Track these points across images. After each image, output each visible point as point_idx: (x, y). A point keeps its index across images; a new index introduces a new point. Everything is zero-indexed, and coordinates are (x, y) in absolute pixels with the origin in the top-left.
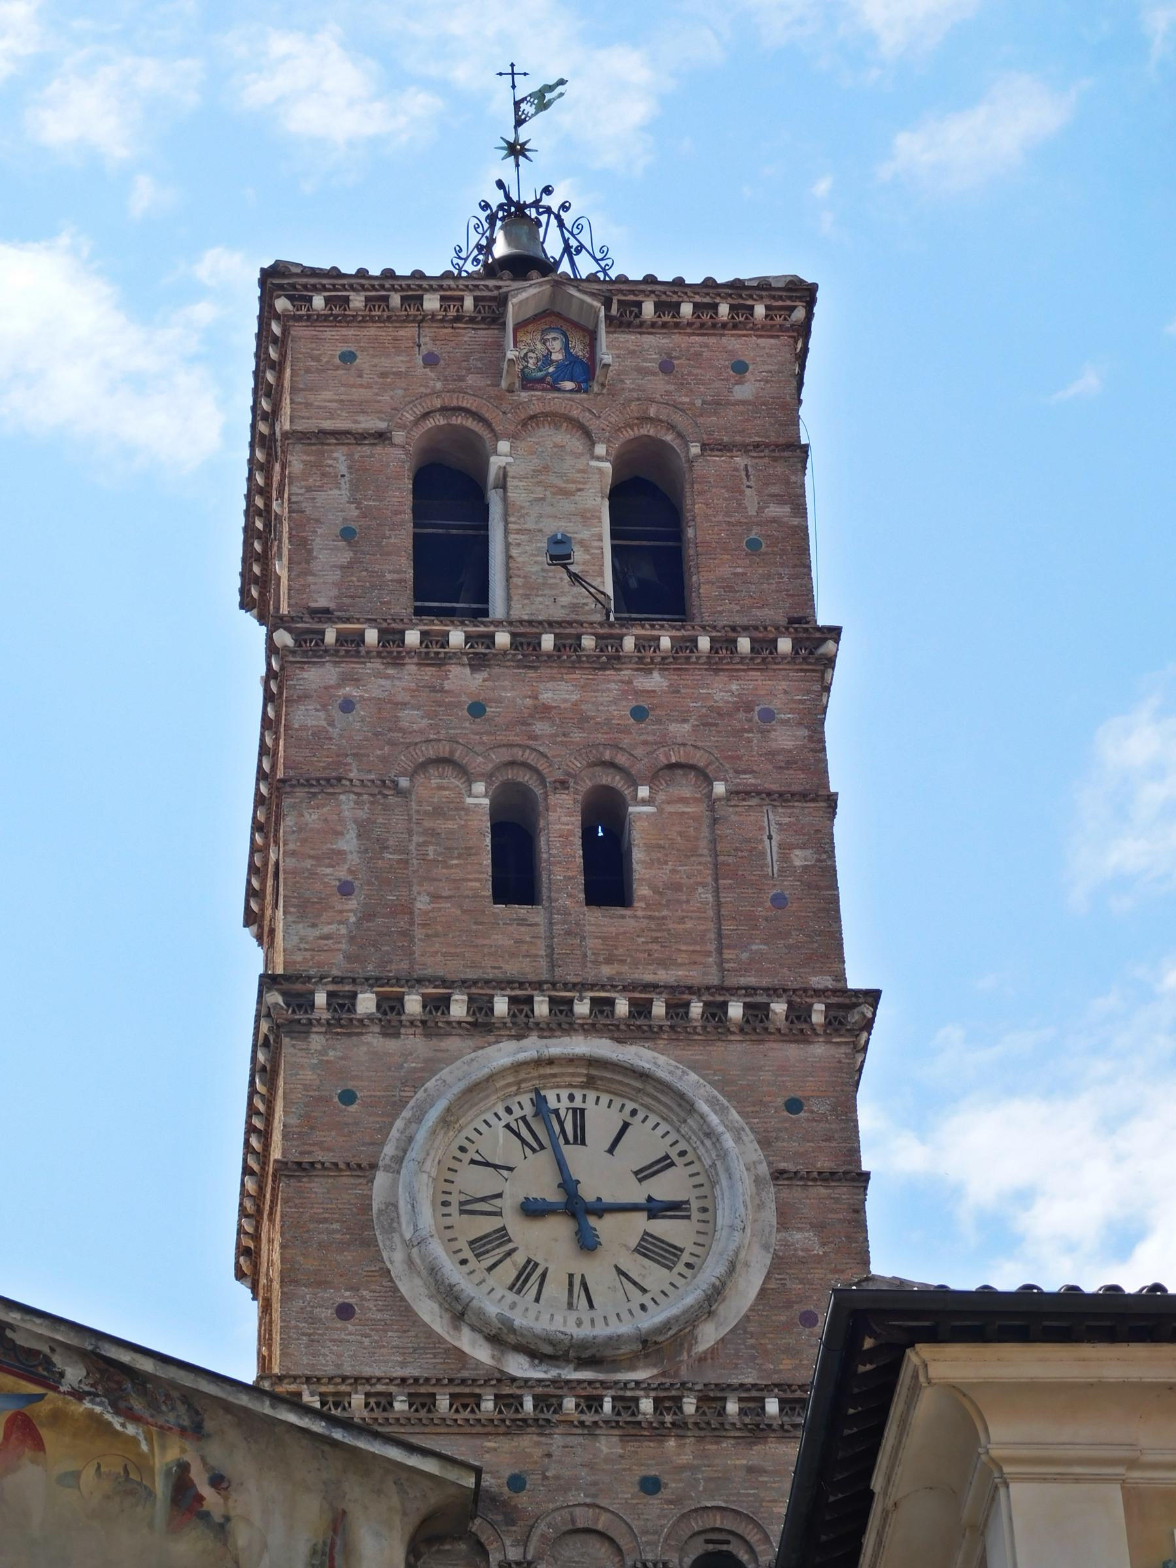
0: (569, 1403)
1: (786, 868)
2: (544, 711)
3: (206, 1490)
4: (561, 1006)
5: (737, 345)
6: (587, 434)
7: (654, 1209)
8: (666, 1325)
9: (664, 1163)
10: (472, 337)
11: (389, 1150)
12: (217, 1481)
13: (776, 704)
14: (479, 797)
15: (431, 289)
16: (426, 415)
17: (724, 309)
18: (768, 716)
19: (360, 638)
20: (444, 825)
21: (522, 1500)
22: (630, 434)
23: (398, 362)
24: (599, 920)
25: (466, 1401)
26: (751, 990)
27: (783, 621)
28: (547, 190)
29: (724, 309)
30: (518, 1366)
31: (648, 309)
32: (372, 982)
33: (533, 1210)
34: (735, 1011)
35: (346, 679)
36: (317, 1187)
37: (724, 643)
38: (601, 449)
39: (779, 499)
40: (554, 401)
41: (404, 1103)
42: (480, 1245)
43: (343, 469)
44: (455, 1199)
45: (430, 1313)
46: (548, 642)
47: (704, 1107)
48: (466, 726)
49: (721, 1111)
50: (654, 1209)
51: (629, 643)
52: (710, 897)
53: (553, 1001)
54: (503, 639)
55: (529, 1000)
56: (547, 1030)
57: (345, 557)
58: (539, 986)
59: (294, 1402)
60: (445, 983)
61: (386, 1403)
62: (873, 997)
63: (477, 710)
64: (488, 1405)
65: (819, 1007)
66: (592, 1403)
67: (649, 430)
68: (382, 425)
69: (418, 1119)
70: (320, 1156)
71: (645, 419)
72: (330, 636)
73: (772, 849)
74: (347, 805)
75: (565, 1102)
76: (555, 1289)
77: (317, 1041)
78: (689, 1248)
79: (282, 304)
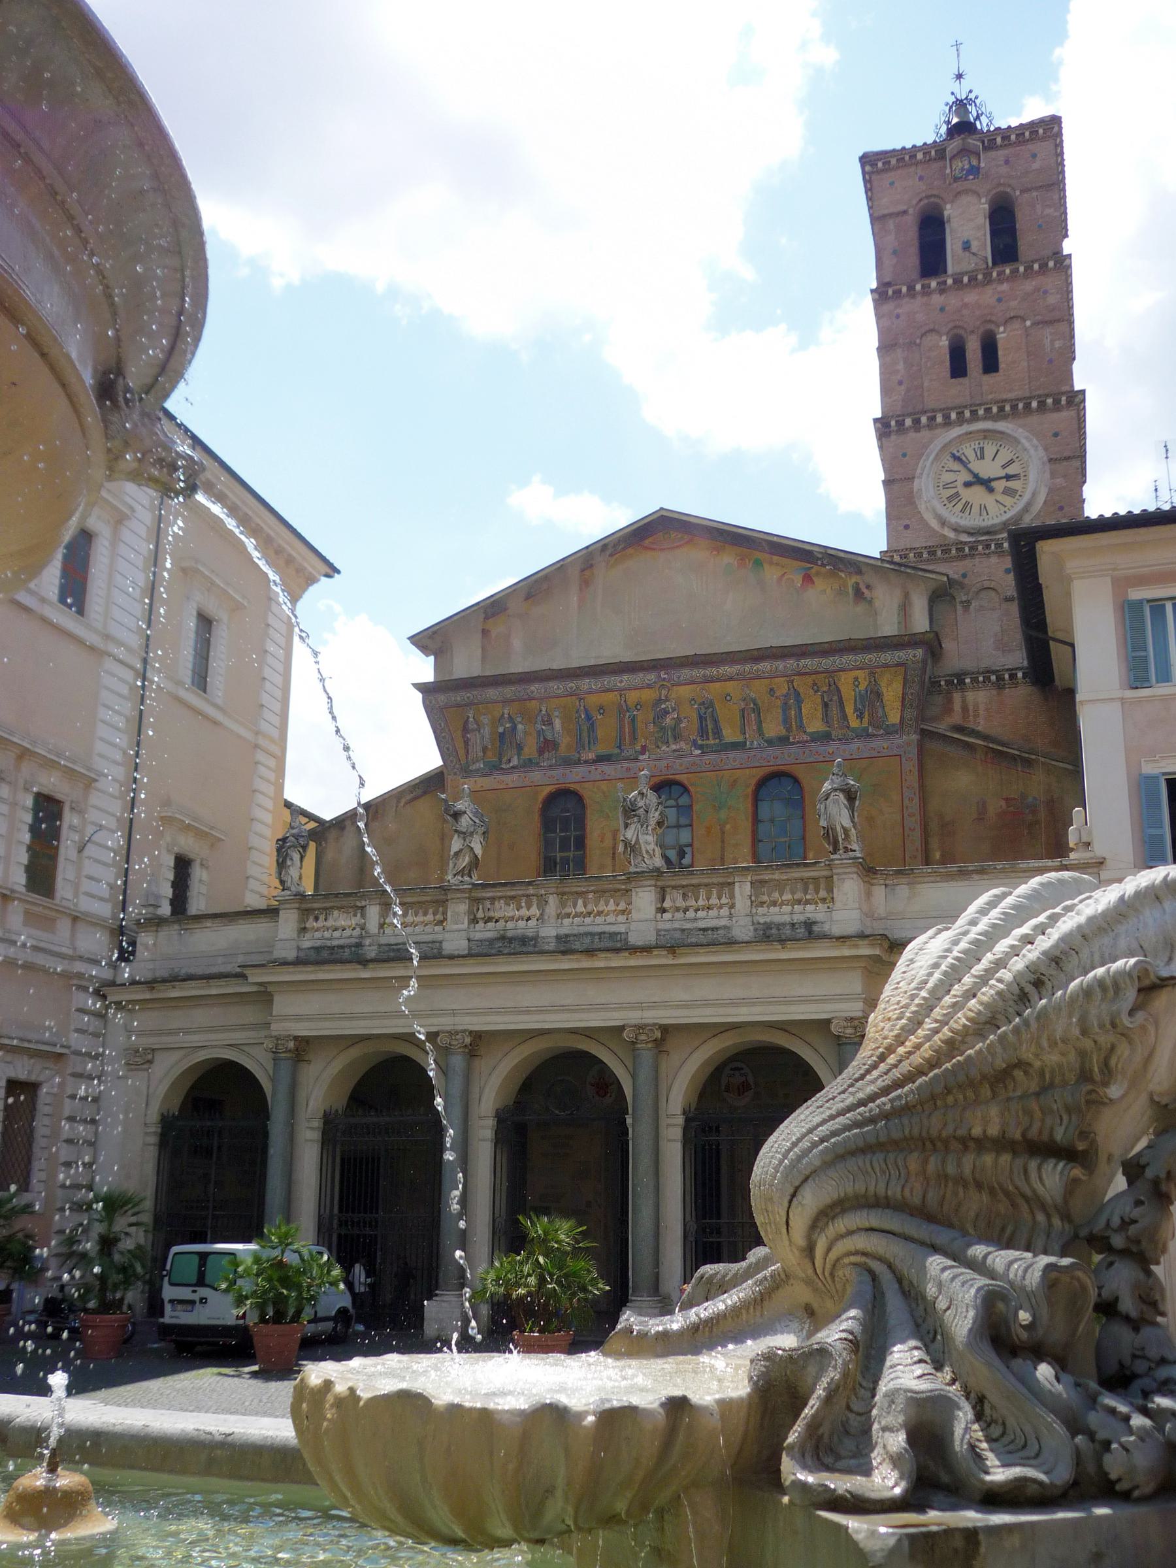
0: (980, 548)
2: (966, 305)
3: (865, 590)
4: (974, 413)
5: (1031, 147)
6: (978, 195)
7: (1008, 477)
8: (1011, 518)
9: (1011, 462)
10: (936, 165)
11: (919, 471)
12: (868, 587)
14: (944, 342)
15: (919, 151)
16: (921, 200)
17: (1027, 134)
18: (1045, 292)
19: (900, 291)
21: (966, 581)
22: (994, 192)
24: (989, 379)
25: (946, 551)
26: (1039, 396)
27: (1051, 254)
28: (971, 91)
29: (1027, 134)
30: (965, 538)
31: (999, 140)
32: (909, 415)
33: (967, 485)
34: (1034, 404)
36: (896, 487)
37: (1029, 268)
38: (983, 200)
39: (1049, 206)
40: (966, 185)
42: (950, 499)
43: (892, 227)
44: (941, 485)
46: (966, 279)
47: (1023, 441)
49: (1030, 440)
50: (1008, 477)
51: (995, 274)
52: (1026, 364)
53: (971, 411)
54: (950, 281)
55: (963, 412)
56: (969, 421)
57: (895, 261)
58: (965, 407)
60: (933, 411)
61: (920, 555)
63: (942, 310)
64: (954, 552)
65: (1064, 399)
66: (988, 546)
67: (1001, 189)
68: (902, 208)
69: (928, 459)
70: (897, 477)
71: (1000, 184)
72: (890, 292)
73: (1047, 342)
74: (899, 351)
75: (977, 446)
76: (976, 509)
77: (893, 437)
78: (1020, 490)
79: (868, 168)
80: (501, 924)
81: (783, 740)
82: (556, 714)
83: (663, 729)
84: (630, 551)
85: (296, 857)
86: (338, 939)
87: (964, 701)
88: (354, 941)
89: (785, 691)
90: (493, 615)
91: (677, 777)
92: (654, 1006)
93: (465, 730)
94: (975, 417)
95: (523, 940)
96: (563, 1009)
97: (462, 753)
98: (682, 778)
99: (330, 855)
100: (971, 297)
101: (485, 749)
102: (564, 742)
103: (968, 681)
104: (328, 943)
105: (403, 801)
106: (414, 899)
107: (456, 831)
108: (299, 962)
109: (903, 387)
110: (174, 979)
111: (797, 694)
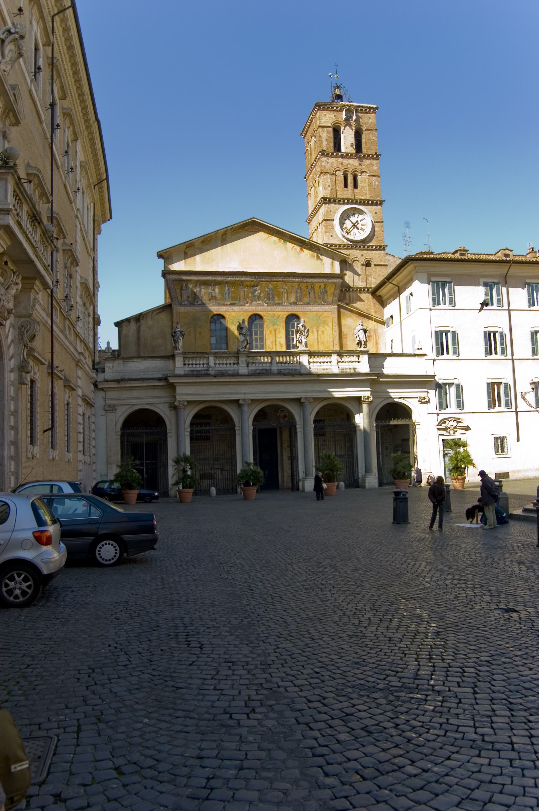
1: (375, 185)
2: (349, 164)
4: (352, 201)
13: (374, 163)
18: (373, 165)
20: (339, 178)
23: (331, 116)
24: (355, 190)
34: (370, 202)
35: (328, 159)
36: (328, 222)
41: (336, 212)
45: (341, 237)
48: (341, 166)
52: (367, 188)
54: (345, 155)
59: (327, 246)
62: (384, 201)
63: (342, 163)
66: (357, 247)
73: (373, 182)
74: (328, 175)
77: (327, 205)
80: (257, 365)
81: (295, 304)
82: (217, 287)
83: (255, 296)
84: (240, 230)
85: (181, 339)
86: (199, 368)
87: (349, 296)
88: (205, 369)
89: (297, 287)
90: (189, 247)
91: (259, 313)
92: (310, 392)
93: (181, 289)
94: (352, 203)
95: (266, 370)
96: (281, 393)
97: (179, 297)
98: (261, 313)
99: (124, 332)
100: (351, 161)
101: (188, 297)
102: (219, 297)
103: (351, 290)
104: (195, 369)
105: (154, 313)
106: (226, 355)
107: (242, 334)
108: (185, 376)
109: (330, 188)
110: (124, 380)
111: (301, 289)
